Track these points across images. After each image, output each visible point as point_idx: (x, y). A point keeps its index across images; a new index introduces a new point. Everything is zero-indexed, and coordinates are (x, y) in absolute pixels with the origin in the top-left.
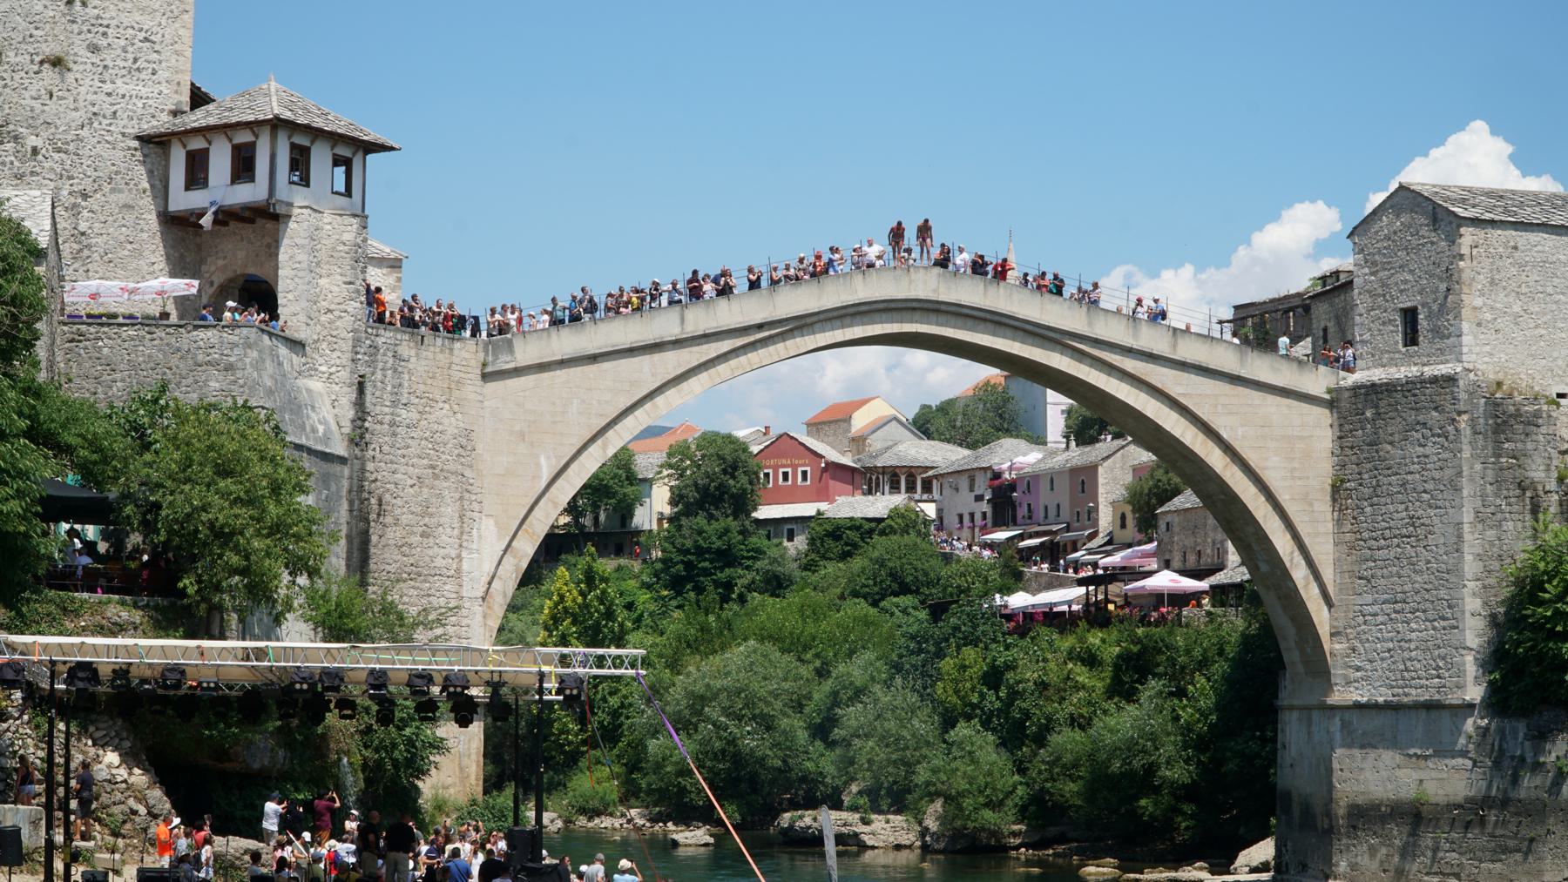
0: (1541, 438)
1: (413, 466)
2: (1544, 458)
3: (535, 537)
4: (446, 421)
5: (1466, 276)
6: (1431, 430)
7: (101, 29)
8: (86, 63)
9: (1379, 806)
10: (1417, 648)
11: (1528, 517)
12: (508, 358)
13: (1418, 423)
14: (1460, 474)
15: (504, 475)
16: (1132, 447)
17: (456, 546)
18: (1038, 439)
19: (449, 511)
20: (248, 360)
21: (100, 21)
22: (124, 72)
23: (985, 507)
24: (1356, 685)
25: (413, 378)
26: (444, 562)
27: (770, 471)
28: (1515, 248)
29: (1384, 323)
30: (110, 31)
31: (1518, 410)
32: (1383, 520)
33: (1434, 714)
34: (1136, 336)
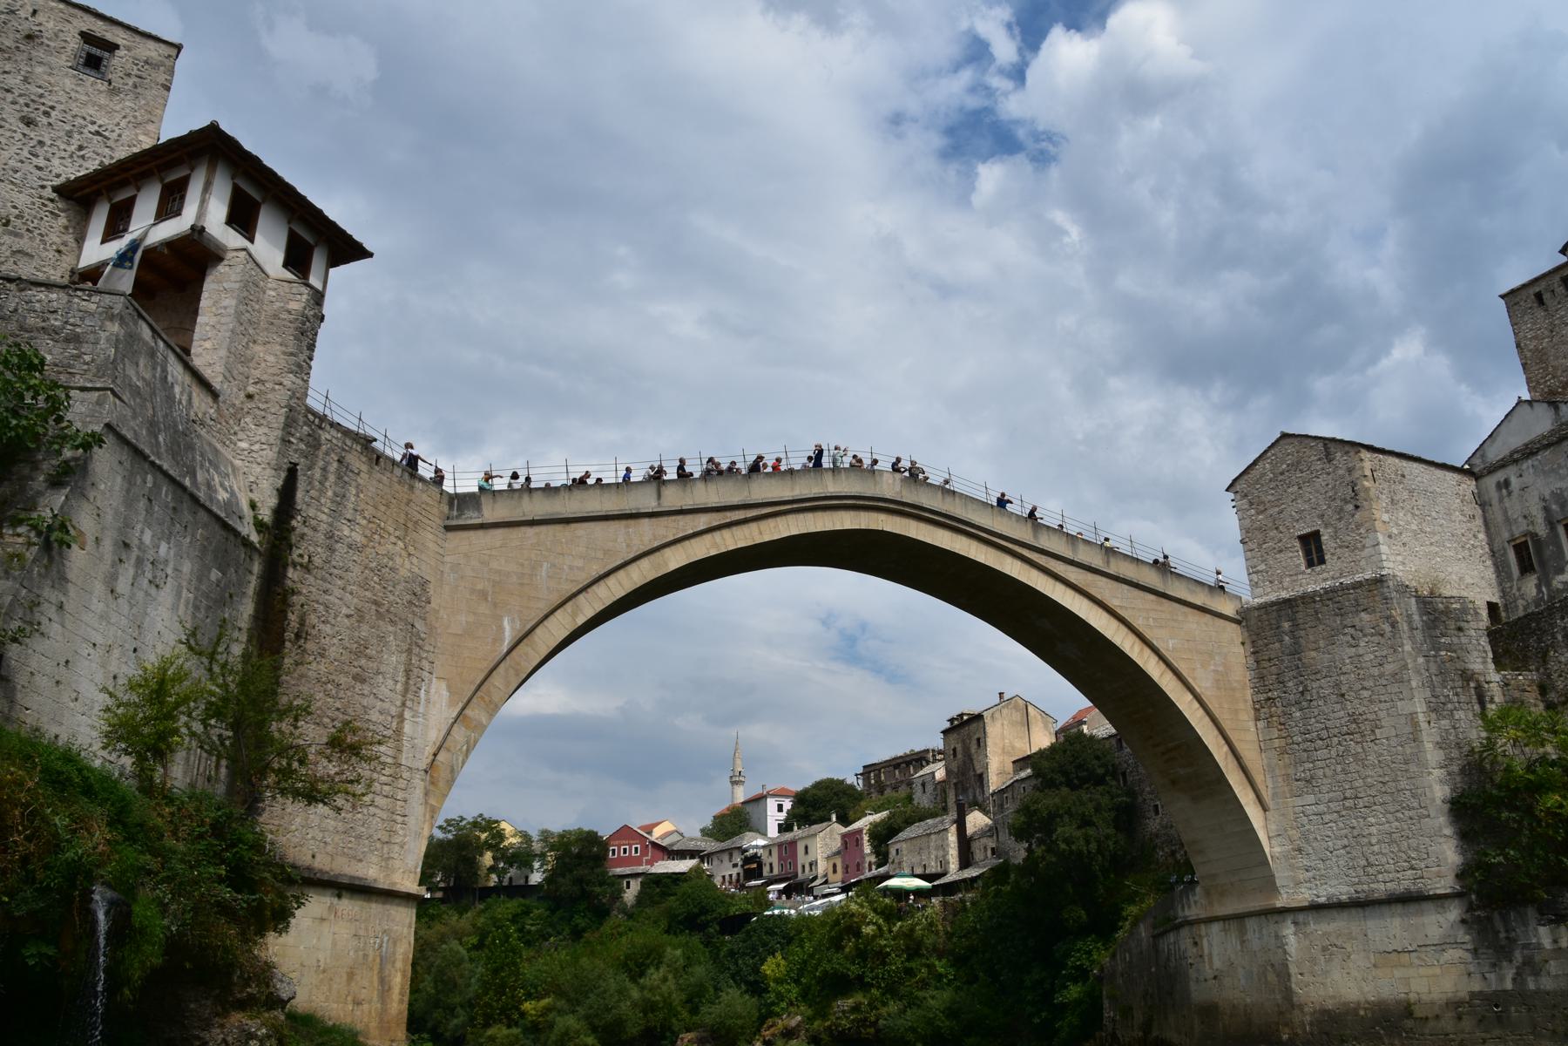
0: (1473, 633)
1: (351, 593)
2: (1479, 651)
3: (492, 706)
4: (398, 560)
5: (1373, 493)
6: (1361, 631)
7: (43, 108)
8: (15, 132)
9: (1356, 1010)
10: (1379, 842)
11: (1477, 707)
12: (476, 514)
13: (1346, 626)
14: (1405, 667)
15: (461, 635)
16: (836, 825)
17: (398, 703)
18: (764, 834)
19: (393, 660)
20: (103, 335)
21: (42, 100)
22: (63, 154)
23: (738, 870)
24: (1308, 885)
25: (362, 495)
26: (382, 718)
28: (1403, 476)
29: (1280, 551)
30: (53, 114)
31: (1447, 607)
32: (1317, 722)
33: (1413, 907)
34: (1075, 550)
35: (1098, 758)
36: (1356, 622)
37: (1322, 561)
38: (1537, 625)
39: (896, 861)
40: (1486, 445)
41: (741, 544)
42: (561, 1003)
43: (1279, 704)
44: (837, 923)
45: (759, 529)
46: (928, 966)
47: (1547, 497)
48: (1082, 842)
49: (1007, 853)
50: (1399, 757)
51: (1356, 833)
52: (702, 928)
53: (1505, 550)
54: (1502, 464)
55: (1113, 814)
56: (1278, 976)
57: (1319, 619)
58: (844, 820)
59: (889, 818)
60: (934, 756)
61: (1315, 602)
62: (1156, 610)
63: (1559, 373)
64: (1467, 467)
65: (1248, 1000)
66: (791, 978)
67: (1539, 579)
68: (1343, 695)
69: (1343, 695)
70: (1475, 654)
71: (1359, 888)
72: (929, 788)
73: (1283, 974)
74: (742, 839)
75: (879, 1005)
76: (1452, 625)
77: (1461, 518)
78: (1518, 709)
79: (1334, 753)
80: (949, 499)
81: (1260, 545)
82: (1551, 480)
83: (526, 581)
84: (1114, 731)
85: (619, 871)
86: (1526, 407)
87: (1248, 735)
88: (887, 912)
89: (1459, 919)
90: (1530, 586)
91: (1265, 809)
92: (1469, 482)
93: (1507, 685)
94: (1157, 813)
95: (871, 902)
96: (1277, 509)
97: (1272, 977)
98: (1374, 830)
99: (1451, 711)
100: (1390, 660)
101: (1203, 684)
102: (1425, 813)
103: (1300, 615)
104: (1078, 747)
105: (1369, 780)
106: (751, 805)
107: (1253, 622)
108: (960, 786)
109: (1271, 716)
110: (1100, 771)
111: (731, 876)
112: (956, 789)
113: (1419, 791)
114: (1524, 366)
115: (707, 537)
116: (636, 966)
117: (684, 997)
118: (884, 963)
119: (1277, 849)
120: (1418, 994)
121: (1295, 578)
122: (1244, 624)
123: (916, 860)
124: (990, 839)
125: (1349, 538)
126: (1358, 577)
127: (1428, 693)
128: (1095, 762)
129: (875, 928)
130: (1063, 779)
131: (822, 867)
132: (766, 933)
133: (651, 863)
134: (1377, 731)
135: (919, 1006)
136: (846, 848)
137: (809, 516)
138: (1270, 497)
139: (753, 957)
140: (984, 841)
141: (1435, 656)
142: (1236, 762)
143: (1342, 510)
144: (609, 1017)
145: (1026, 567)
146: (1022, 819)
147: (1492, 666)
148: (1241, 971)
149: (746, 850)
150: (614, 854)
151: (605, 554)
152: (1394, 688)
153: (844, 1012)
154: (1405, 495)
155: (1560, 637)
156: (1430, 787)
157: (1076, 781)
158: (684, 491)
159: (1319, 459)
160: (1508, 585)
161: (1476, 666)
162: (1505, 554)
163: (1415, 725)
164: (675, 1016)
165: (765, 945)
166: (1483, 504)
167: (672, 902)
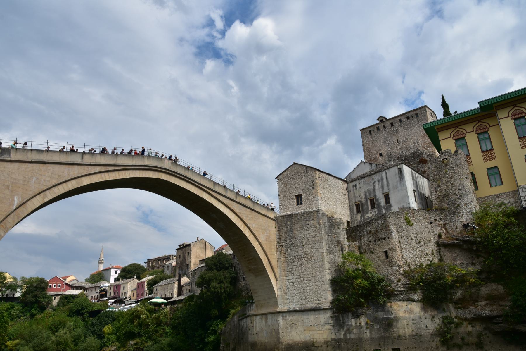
0: (342, 229)
5: (318, 184)
9: (298, 344)
10: (309, 292)
11: (341, 252)
12: (8, 156)
13: (306, 224)
14: (322, 238)
16: (136, 280)
23: (98, 294)
24: (287, 304)
27: (51, 285)
28: (327, 180)
29: (290, 199)
31: (335, 221)
33: (317, 312)
34: (226, 192)
35: (227, 261)
36: (309, 223)
37: (301, 204)
38: (360, 228)
39: (156, 293)
40: (351, 174)
41: (111, 179)
42: (23, 342)
43: (284, 247)
44: (132, 314)
45: (119, 174)
46: (163, 329)
47: (366, 191)
48: (219, 288)
49: (194, 291)
50: (318, 266)
51: (303, 289)
52: (82, 315)
53: (353, 205)
54: (355, 180)
55: (230, 280)
56: (276, 333)
57: (299, 221)
58: (139, 278)
59: (155, 278)
60: (173, 257)
61: (298, 216)
62: (250, 214)
63: (373, 155)
64: (345, 179)
65: (266, 341)
66: (114, 333)
67: (361, 215)
68: (303, 246)
69: (303, 246)
70: (342, 236)
71: (302, 306)
72: (170, 268)
73: (278, 333)
74: (101, 283)
75: (144, 343)
76: (336, 226)
77: (342, 194)
78: (353, 253)
79: (299, 263)
80: (187, 171)
81: (284, 197)
82: (368, 186)
83: (26, 183)
84: (233, 253)
85: (52, 293)
86: (363, 164)
87: (274, 256)
88: (151, 310)
89: (330, 316)
90: (359, 217)
91: (277, 280)
92: (345, 184)
93: (350, 246)
94: (244, 280)
95: (145, 307)
96: (290, 186)
97: (274, 333)
98: (308, 288)
99: (334, 253)
100: (318, 236)
101: (262, 239)
102: (323, 283)
103: (293, 220)
104: (221, 257)
105: (308, 272)
106: (105, 271)
107: (279, 221)
108: (180, 268)
109: (282, 251)
110: (227, 265)
111: (95, 296)
112: (179, 269)
113: (322, 277)
114: (364, 151)
115: (99, 175)
116: (54, 328)
117: (72, 340)
118: (148, 328)
119: (279, 293)
120: (317, 339)
121: (293, 208)
122: (276, 221)
123: (163, 292)
124: (189, 287)
125: (310, 197)
126: (311, 210)
127: (328, 247)
128: (226, 262)
129: (146, 316)
130: (215, 268)
131: (129, 294)
132: (106, 317)
133: (64, 291)
134: (312, 257)
135: (159, 343)
136: (138, 288)
137: (138, 171)
138: (288, 182)
139: (100, 326)
140: (187, 287)
141: (331, 236)
142: (269, 265)
143: (309, 188)
144: (42, 347)
145: (210, 196)
146: (200, 280)
147: (346, 240)
148: (265, 332)
149: (102, 287)
150: (50, 287)
151: (59, 177)
152: (318, 245)
153: (132, 345)
154: (327, 186)
155: (365, 233)
156: (325, 275)
157: (219, 268)
158: (92, 157)
159: (304, 172)
160: (353, 216)
161: (342, 240)
162: (353, 207)
163: (323, 256)
164: (68, 346)
165: (105, 321)
166: (349, 191)
167: (71, 305)
